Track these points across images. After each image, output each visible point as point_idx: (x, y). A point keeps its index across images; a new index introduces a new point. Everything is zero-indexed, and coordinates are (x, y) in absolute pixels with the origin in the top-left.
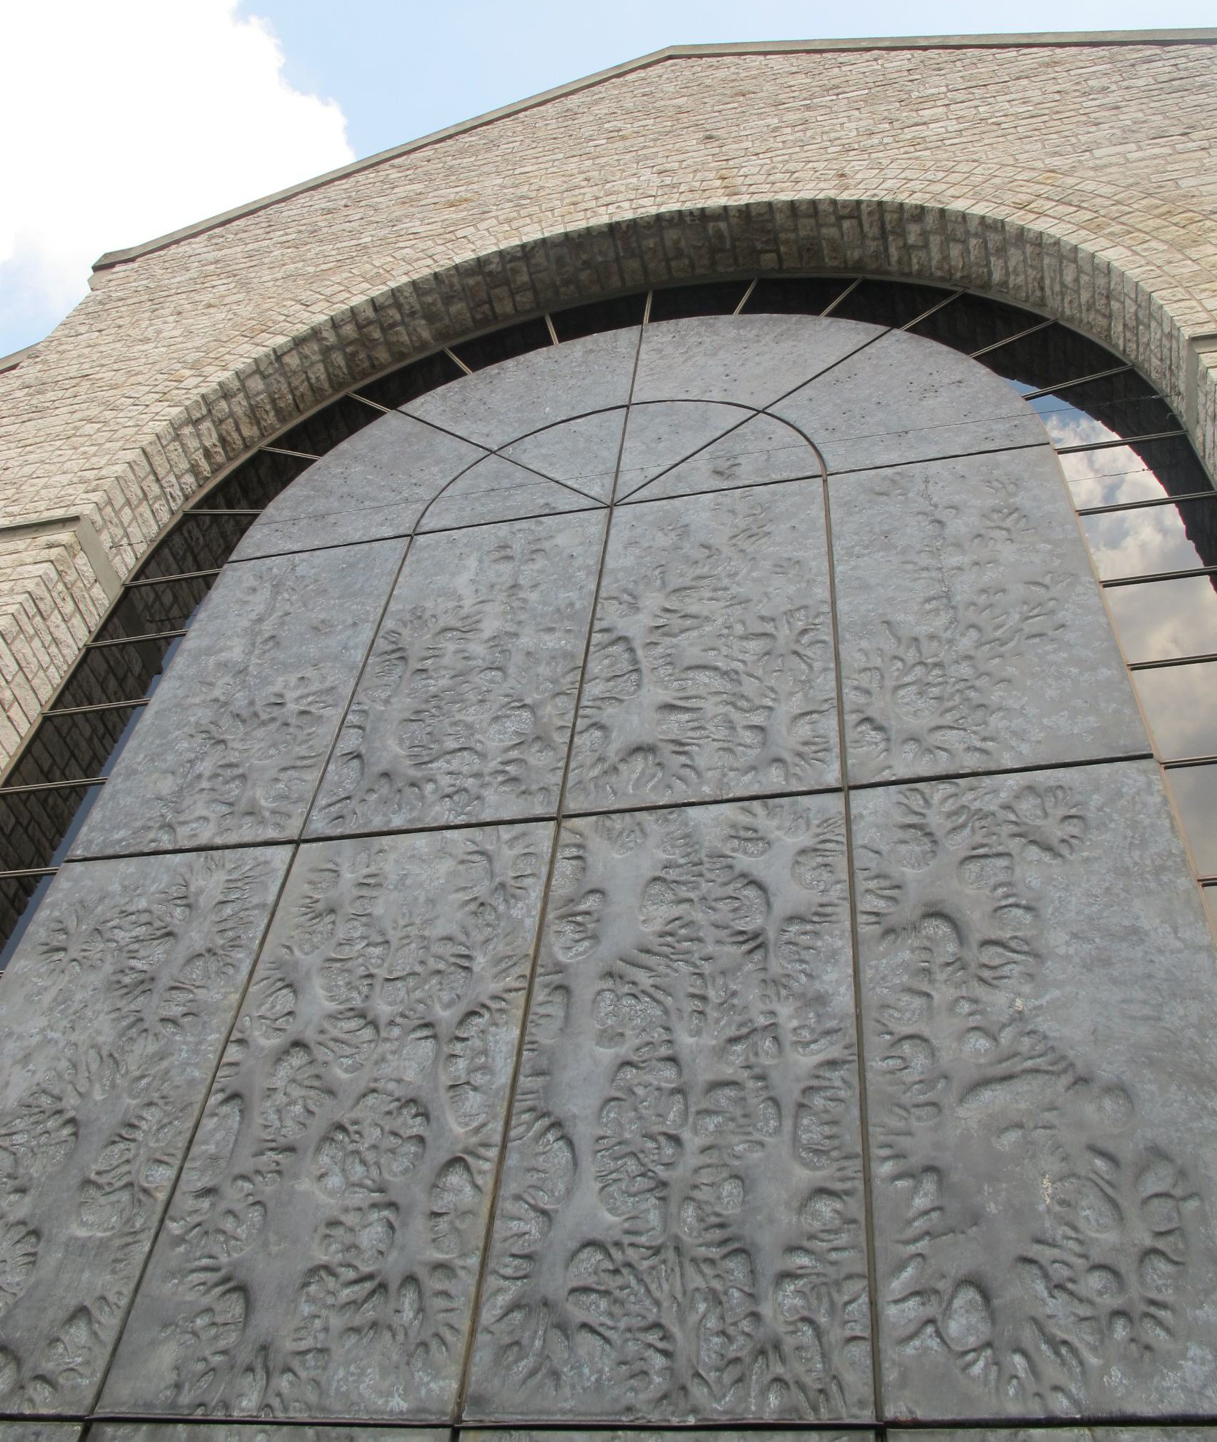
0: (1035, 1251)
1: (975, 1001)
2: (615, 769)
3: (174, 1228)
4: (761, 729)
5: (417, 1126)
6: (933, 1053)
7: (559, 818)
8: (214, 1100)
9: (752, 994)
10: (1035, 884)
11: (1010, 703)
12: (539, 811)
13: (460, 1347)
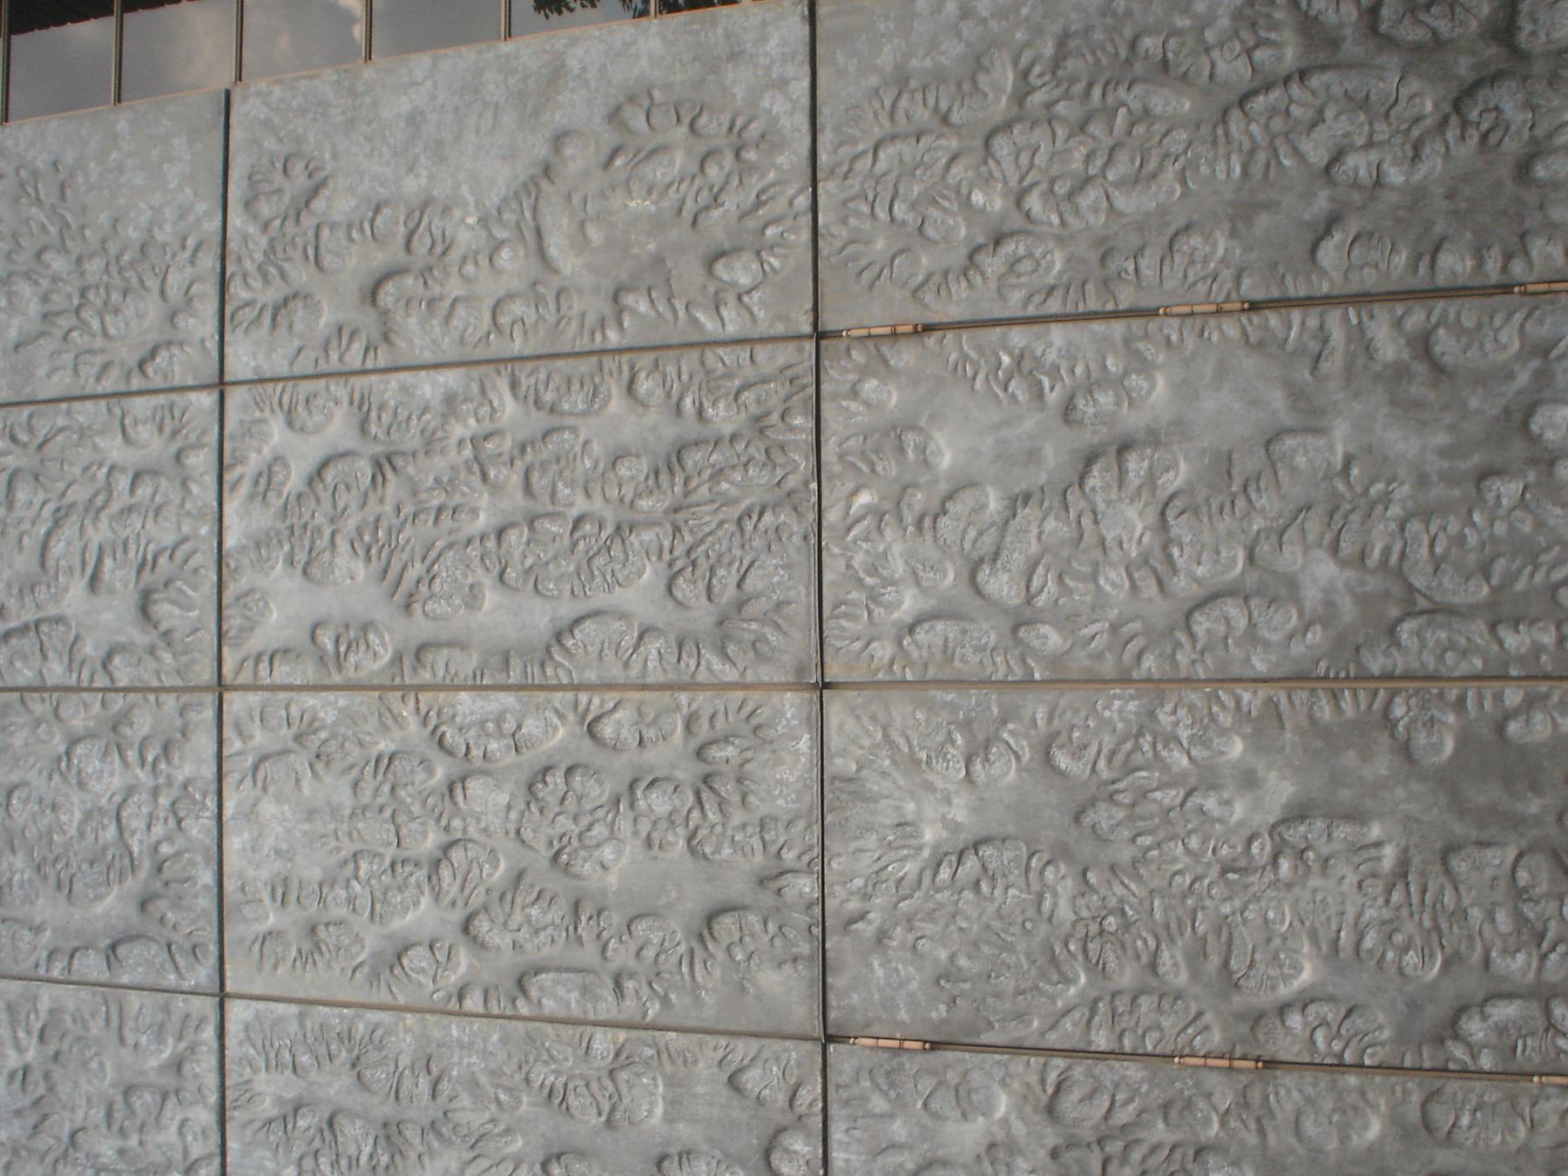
0: (687, 214)
1: (464, 260)
2: (166, 635)
3: (653, 1010)
4: (137, 478)
5: (556, 779)
6: (511, 296)
7: (221, 686)
8: (523, 1008)
9: (440, 464)
10: (353, 202)
11: (144, 220)
12: (209, 713)
13: (756, 696)
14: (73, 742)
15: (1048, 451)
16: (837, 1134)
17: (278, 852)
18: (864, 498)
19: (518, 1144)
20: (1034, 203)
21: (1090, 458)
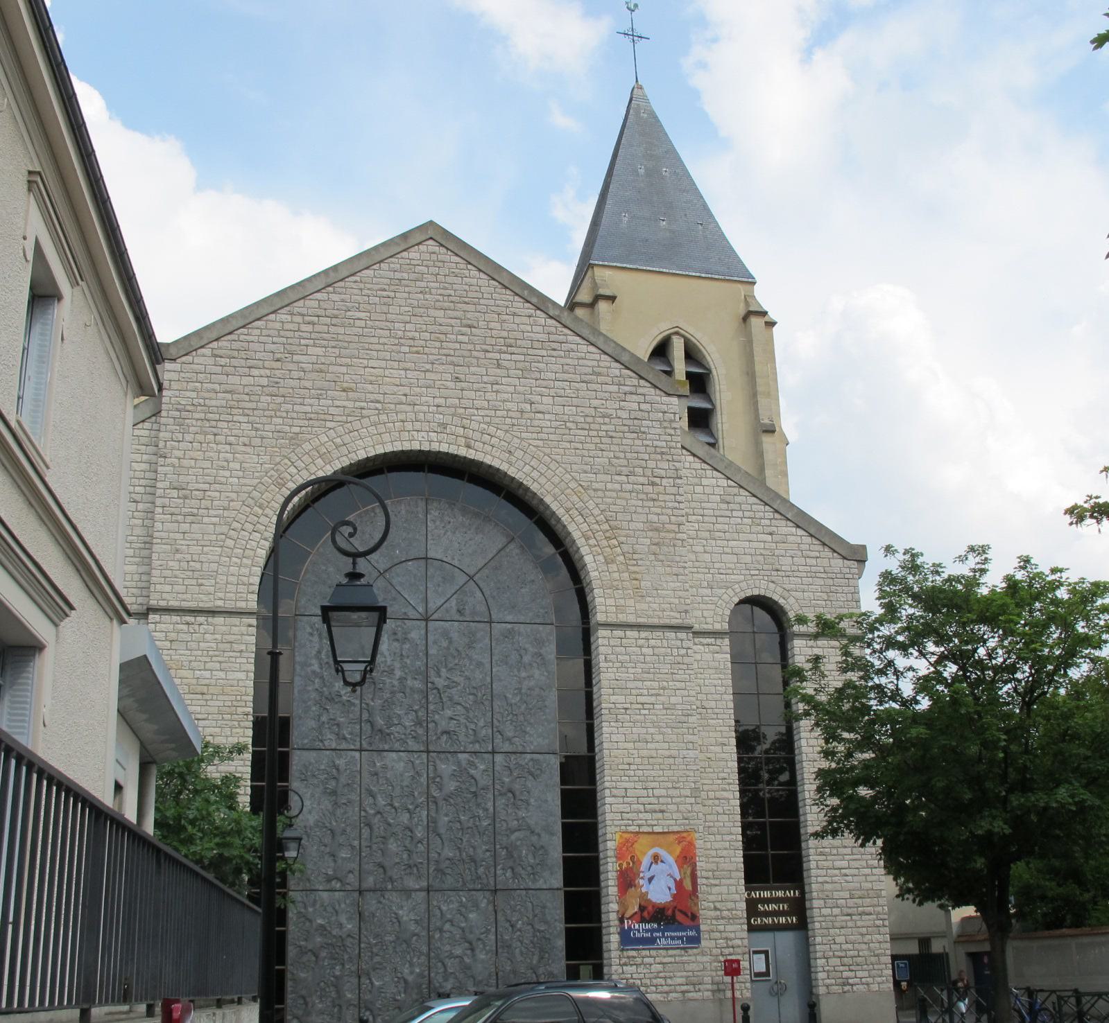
3: (363, 854)
5: (409, 834)
6: (507, 824)
8: (362, 825)
10: (530, 786)
12: (422, 749)
14: (416, 712)
15: (472, 936)
16: (341, 893)
17: (393, 767)
18: (464, 899)
19: (335, 824)
20: (519, 933)
21: (470, 943)
